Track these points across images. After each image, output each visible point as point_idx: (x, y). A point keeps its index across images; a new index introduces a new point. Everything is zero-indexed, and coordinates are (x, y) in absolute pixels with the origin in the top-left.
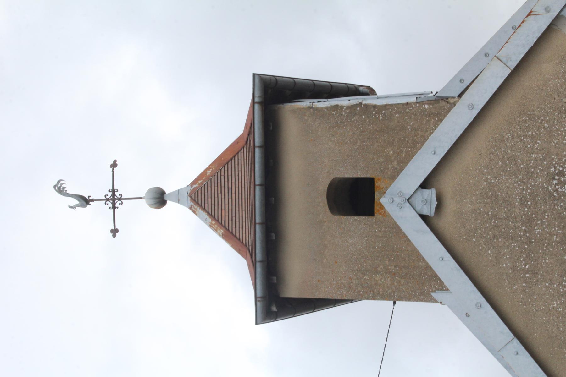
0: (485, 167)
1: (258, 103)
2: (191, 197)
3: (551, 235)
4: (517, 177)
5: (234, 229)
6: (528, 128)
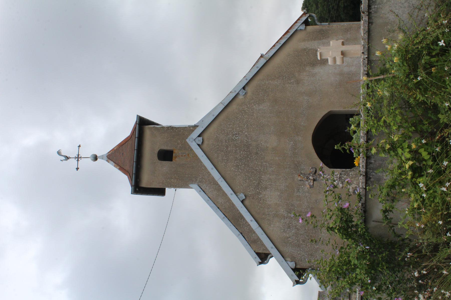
2: (107, 157)
3: (233, 150)
5: (123, 167)
6: (228, 122)
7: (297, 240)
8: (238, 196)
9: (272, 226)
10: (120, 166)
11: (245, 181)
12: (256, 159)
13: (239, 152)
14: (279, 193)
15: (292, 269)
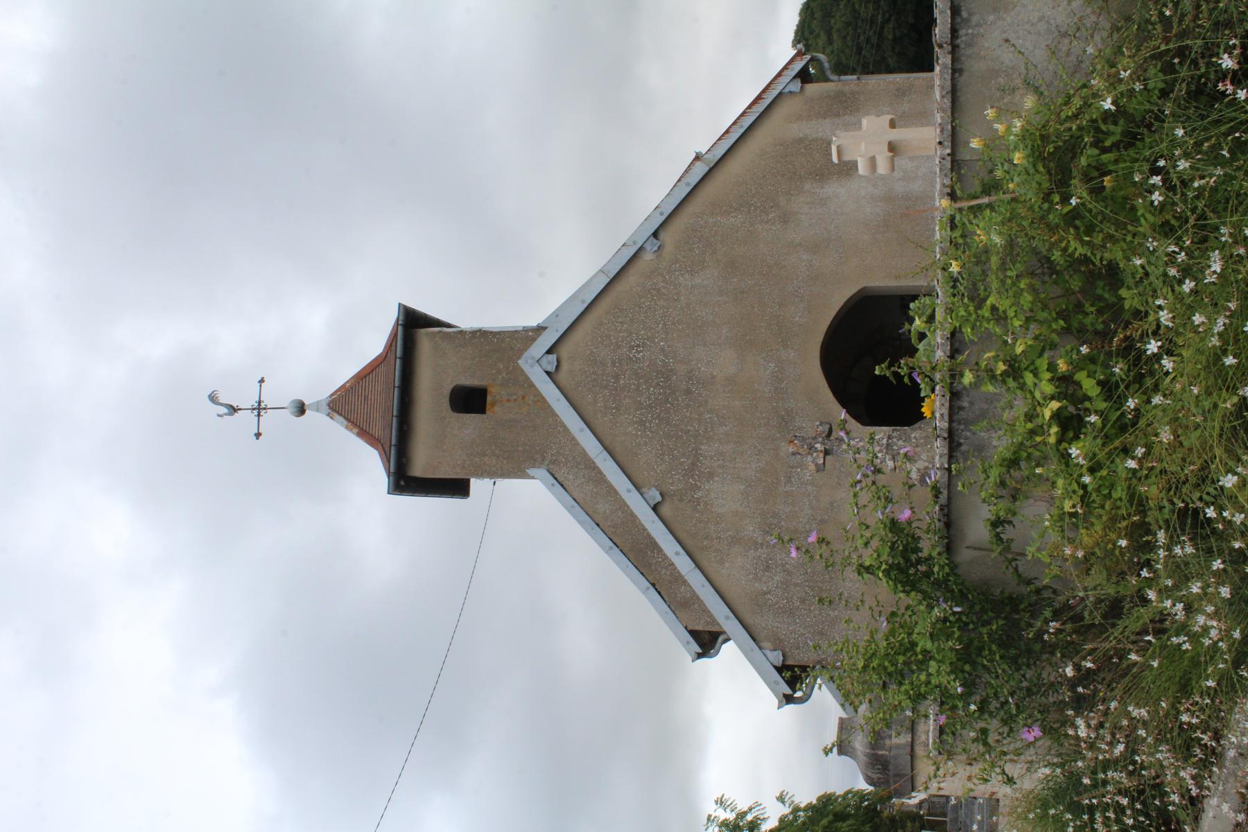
6: (619, 317)
8: (645, 495)
9: (727, 565)
15: (775, 667)
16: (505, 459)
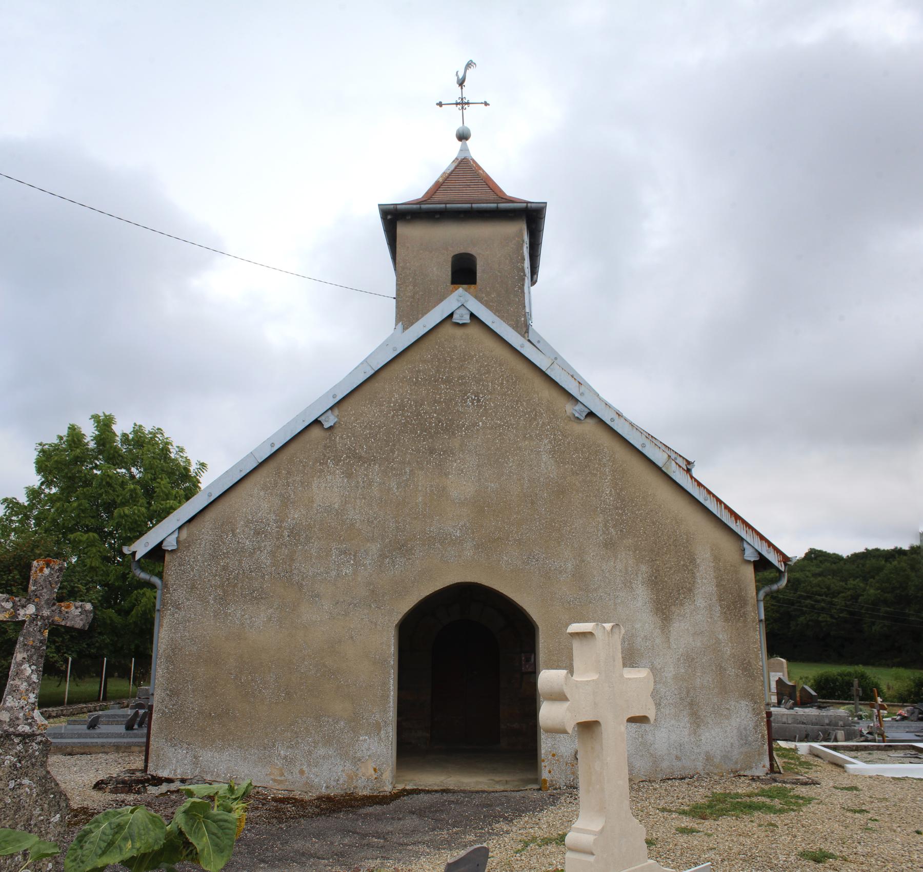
0: (484, 354)
1: (527, 205)
3: (440, 394)
4: (477, 374)
6: (508, 381)
7: (228, 553)
8: (330, 411)
9: (262, 493)
10: (444, 183)
11: (366, 427)
12: (418, 451)
13: (436, 409)
14: (336, 506)
15: (161, 543)
16: (411, 303)
